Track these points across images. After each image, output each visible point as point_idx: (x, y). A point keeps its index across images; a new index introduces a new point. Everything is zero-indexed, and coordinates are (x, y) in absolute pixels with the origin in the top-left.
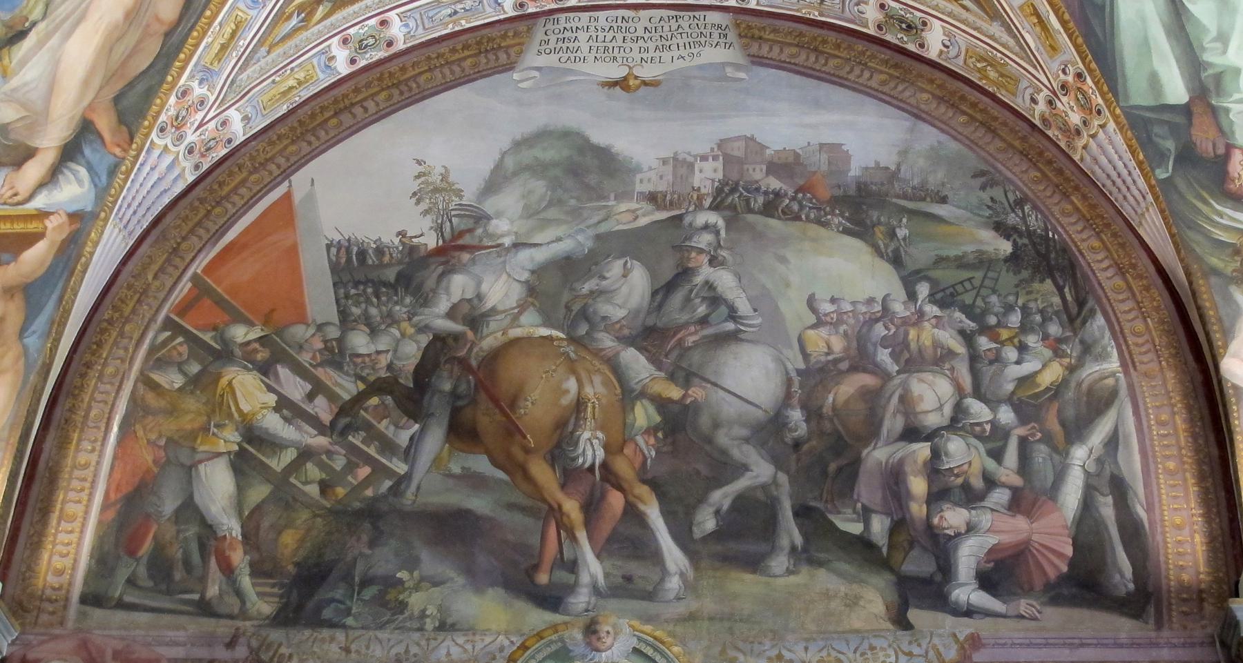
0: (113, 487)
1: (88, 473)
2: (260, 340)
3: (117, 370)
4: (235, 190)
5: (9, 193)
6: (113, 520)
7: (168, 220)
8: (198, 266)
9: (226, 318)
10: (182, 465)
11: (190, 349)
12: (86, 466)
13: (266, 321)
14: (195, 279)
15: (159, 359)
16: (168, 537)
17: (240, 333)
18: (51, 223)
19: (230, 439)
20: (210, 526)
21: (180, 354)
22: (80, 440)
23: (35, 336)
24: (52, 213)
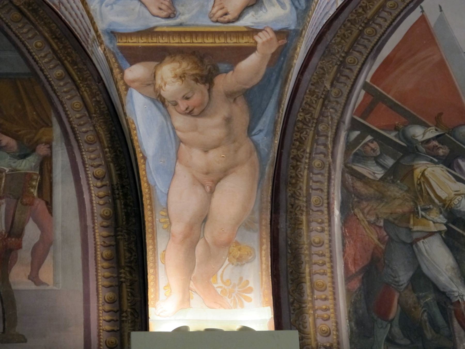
0: (350, 261)
1: (325, 249)
2: (437, 138)
3: (323, 163)
4: (377, 13)
5: (220, 13)
6: (360, 289)
7: (329, 37)
8: (367, 76)
9: (404, 120)
10: (404, 243)
11: (380, 145)
12: (321, 244)
13: (438, 122)
14: (365, 86)
15: (356, 154)
16: (410, 301)
17: (418, 133)
18: (260, 39)
19: (436, 221)
20: (444, 293)
21: (374, 150)
22: (309, 222)
23: (262, 134)
24: (261, 31)
